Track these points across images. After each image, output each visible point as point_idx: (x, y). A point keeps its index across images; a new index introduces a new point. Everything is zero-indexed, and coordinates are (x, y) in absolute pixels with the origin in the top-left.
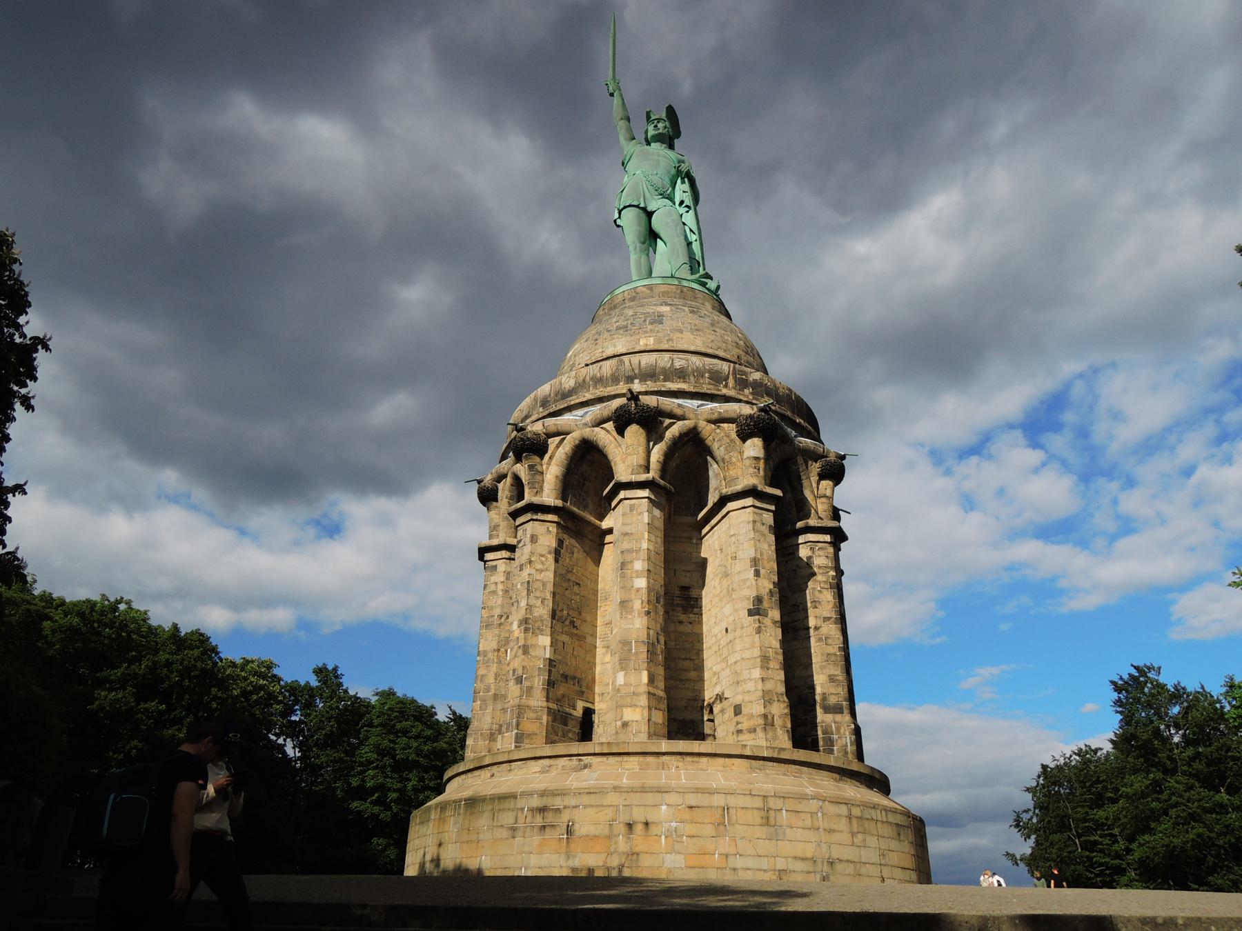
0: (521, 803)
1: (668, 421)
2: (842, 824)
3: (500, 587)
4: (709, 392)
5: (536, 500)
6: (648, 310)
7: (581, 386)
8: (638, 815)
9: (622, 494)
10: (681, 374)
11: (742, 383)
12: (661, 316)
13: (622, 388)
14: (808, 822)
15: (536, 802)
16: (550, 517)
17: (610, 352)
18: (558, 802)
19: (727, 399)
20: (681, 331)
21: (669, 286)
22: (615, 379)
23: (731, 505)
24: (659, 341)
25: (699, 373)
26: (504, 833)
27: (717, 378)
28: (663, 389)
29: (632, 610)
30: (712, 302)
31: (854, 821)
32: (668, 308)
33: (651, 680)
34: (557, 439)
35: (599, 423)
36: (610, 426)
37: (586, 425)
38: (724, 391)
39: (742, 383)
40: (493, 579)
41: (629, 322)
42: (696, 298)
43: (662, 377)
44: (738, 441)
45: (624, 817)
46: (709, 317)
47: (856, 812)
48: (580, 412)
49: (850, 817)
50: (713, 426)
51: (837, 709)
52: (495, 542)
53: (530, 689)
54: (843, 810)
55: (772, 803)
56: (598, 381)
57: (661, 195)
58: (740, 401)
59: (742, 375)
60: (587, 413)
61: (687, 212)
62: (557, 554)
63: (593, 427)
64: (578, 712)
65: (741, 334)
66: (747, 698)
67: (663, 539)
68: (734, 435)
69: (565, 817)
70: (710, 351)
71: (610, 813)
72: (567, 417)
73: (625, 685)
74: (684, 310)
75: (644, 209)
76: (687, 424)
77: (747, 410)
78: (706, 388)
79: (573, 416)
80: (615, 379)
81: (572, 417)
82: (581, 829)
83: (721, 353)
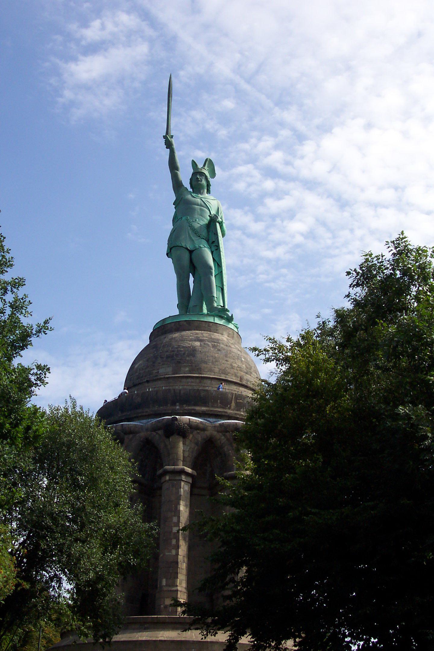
1: (195, 432)
4: (220, 414)
6: (187, 345)
9: (167, 478)
11: (239, 406)
19: (230, 418)
21: (200, 322)
28: (193, 411)
30: (228, 331)
32: (197, 344)
34: (131, 436)
35: (155, 429)
36: (161, 432)
37: (147, 430)
41: (175, 353)
42: (217, 330)
43: (193, 403)
46: (224, 349)
48: (144, 421)
50: (220, 434)
57: (200, 236)
59: (240, 400)
60: (148, 422)
61: (217, 250)
63: (153, 431)
65: (244, 358)
67: (188, 503)
73: (167, 585)
74: (208, 345)
79: (140, 423)
81: (138, 424)
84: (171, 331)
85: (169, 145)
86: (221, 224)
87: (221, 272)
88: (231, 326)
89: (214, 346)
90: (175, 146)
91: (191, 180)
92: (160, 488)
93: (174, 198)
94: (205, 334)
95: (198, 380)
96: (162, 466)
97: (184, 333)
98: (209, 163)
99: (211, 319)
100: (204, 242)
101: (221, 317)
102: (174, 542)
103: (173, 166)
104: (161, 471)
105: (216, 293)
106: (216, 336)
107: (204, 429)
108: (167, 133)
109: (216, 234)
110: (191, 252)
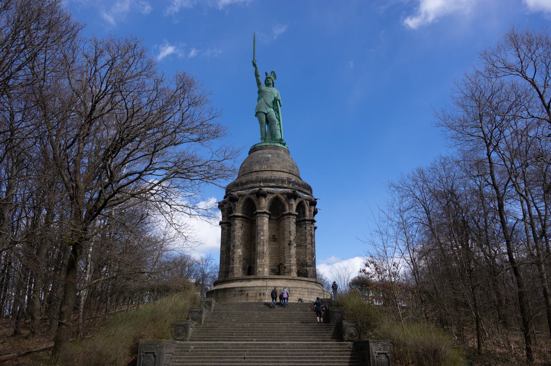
0: (236, 289)
1: (270, 195)
2: (306, 293)
3: (226, 234)
5: (236, 214)
7: (247, 183)
8: (262, 292)
10: (273, 181)
12: (269, 158)
13: (258, 184)
14: (298, 293)
15: (239, 289)
16: (239, 219)
17: (254, 169)
18: (245, 289)
19: (285, 188)
20: (274, 164)
22: (256, 182)
23: (286, 217)
24: (268, 167)
25: (278, 180)
26: (233, 296)
27: (283, 181)
29: (261, 244)
31: (309, 293)
32: (270, 155)
33: (265, 261)
34: (241, 197)
35: (252, 194)
36: (254, 195)
37: (249, 194)
38: (285, 185)
39: (289, 182)
40: (224, 231)
44: (288, 200)
45: (259, 292)
47: (310, 290)
48: (247, 191)
49: (308, 292)
51: (310, 266)
52: (224, 221)
53: (236, 262)
54: (307, 290)
55: (291, 289)
56: (252, 182)
58: (288, 188)
62: (241, 228)
64: (247, 268)
66: (287, 265)
68: (286, 198)
69: (246, 292)
70: (282, 170)
71: (256, 291)
72: (243, 192)
75: (264, 113)
76: (274, 195)
77: (290, 191)
78: (280, 185)
80: (256, 182)
82: (250, 295)
83: (285, 170)
84: (258, 150)
85: (254, 65)
86: (279, 101)
87: (280, 123)
88: (285, 147)
89: (277, 156)
90: (257, 66)
91: (265, 81)
92: (255, 220)
93: (258, 90)
94: (273, 151)
95: (270, 172)
96: (256, 210)
97: (264, 151)
98: (273, 72)
99: (276, 145)
100: (272, 110)
101: (281, 143)
102: (262, 243)
103: (257, 75)
104: (255, 212)
105: (279, 132)
106: (278, 152)
107: (273, 194)
108: (254, 59)
109: (277, 106)
110: (266, 114)
